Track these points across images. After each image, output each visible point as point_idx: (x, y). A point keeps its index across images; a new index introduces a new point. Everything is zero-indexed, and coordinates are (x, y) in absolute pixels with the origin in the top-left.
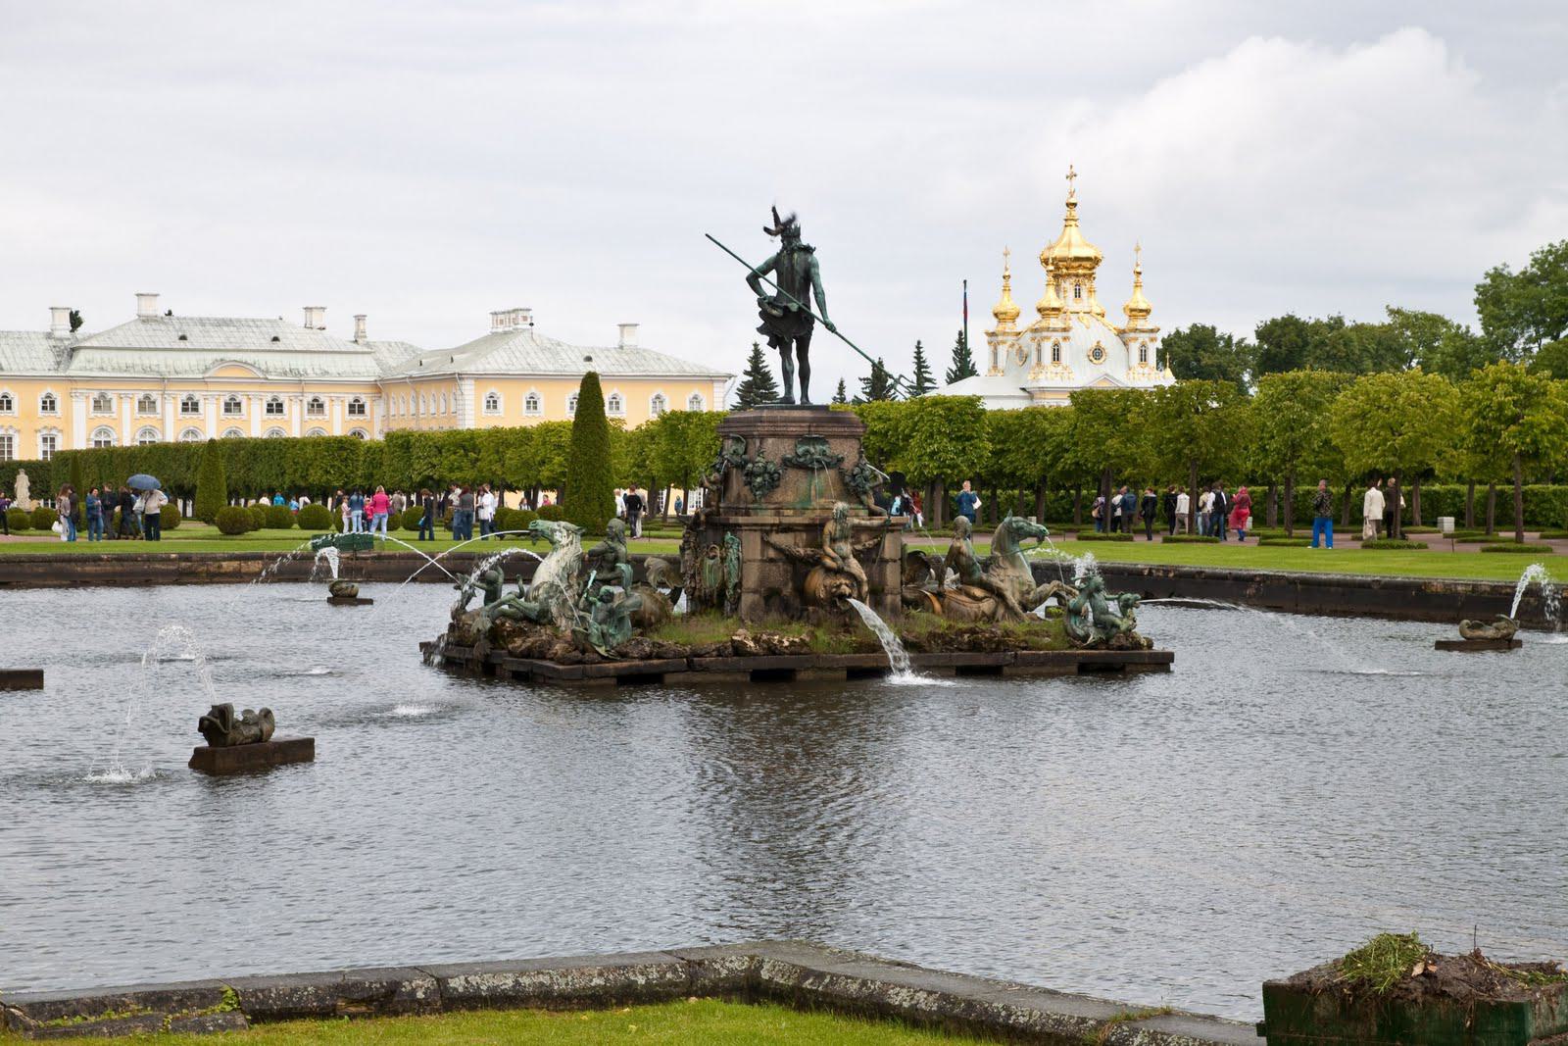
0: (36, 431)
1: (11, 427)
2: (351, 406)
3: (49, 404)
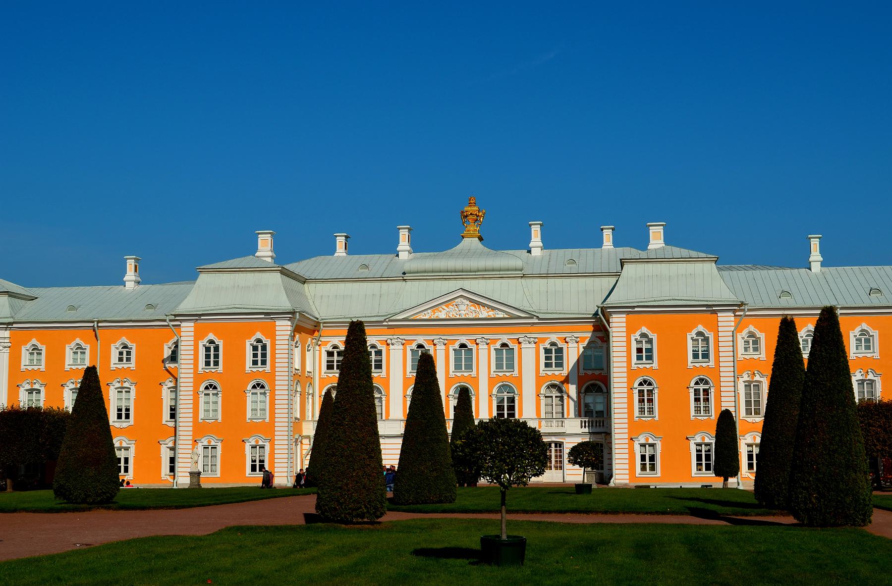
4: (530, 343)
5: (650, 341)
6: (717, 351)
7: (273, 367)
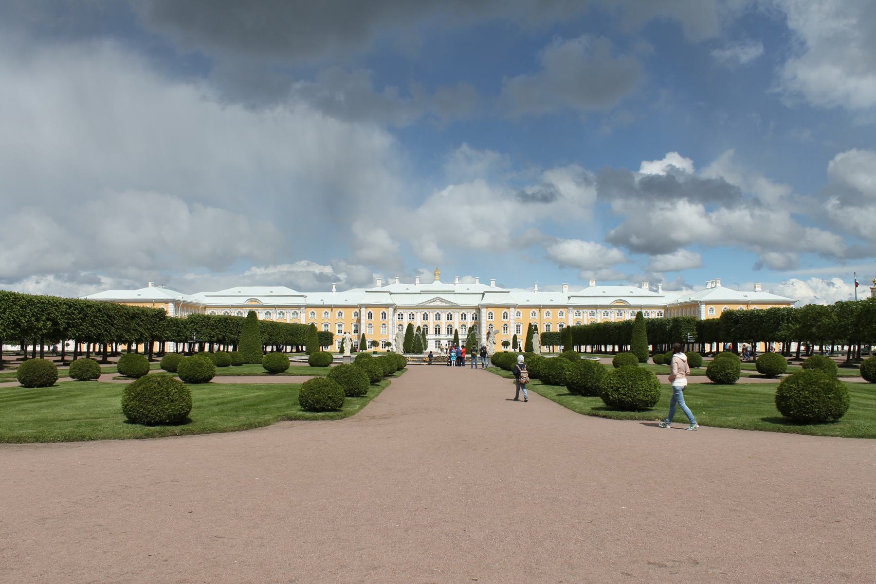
1: (550, 322)
5: (492, 314)
7: (388, 320)
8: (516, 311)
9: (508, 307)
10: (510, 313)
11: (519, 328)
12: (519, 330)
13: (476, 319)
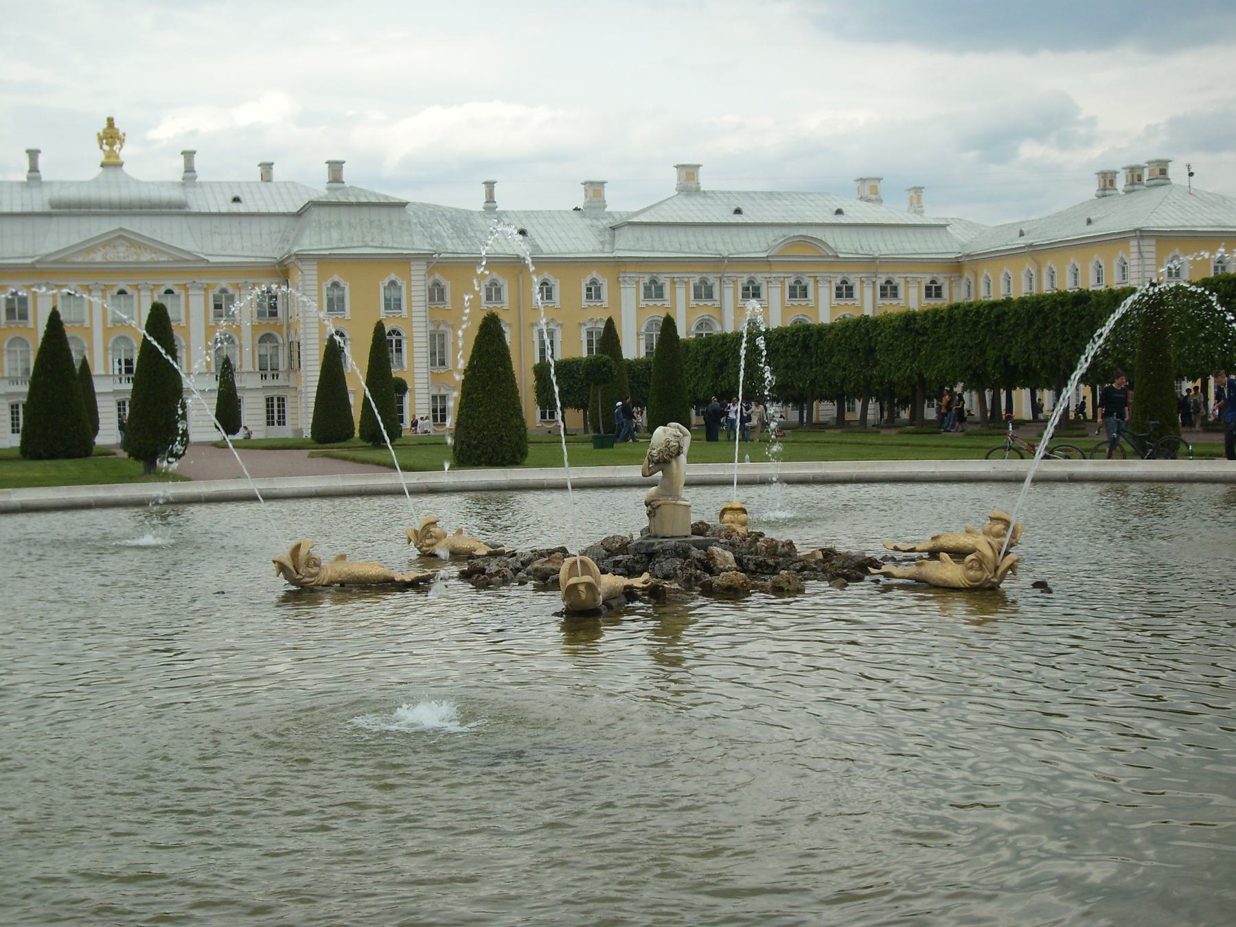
0: (580, 325)
2: (928, 288)
3: (593, 291)
4: (199, 289)
6: (410, 302)
8: (430, 282)
9: (403, 261)
10: (409, 286)
11: (443, 346)
12: (442, 353)
13: (274, 314)
